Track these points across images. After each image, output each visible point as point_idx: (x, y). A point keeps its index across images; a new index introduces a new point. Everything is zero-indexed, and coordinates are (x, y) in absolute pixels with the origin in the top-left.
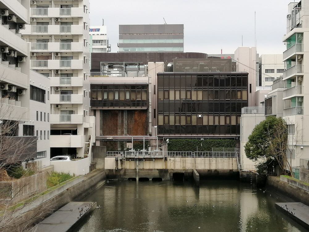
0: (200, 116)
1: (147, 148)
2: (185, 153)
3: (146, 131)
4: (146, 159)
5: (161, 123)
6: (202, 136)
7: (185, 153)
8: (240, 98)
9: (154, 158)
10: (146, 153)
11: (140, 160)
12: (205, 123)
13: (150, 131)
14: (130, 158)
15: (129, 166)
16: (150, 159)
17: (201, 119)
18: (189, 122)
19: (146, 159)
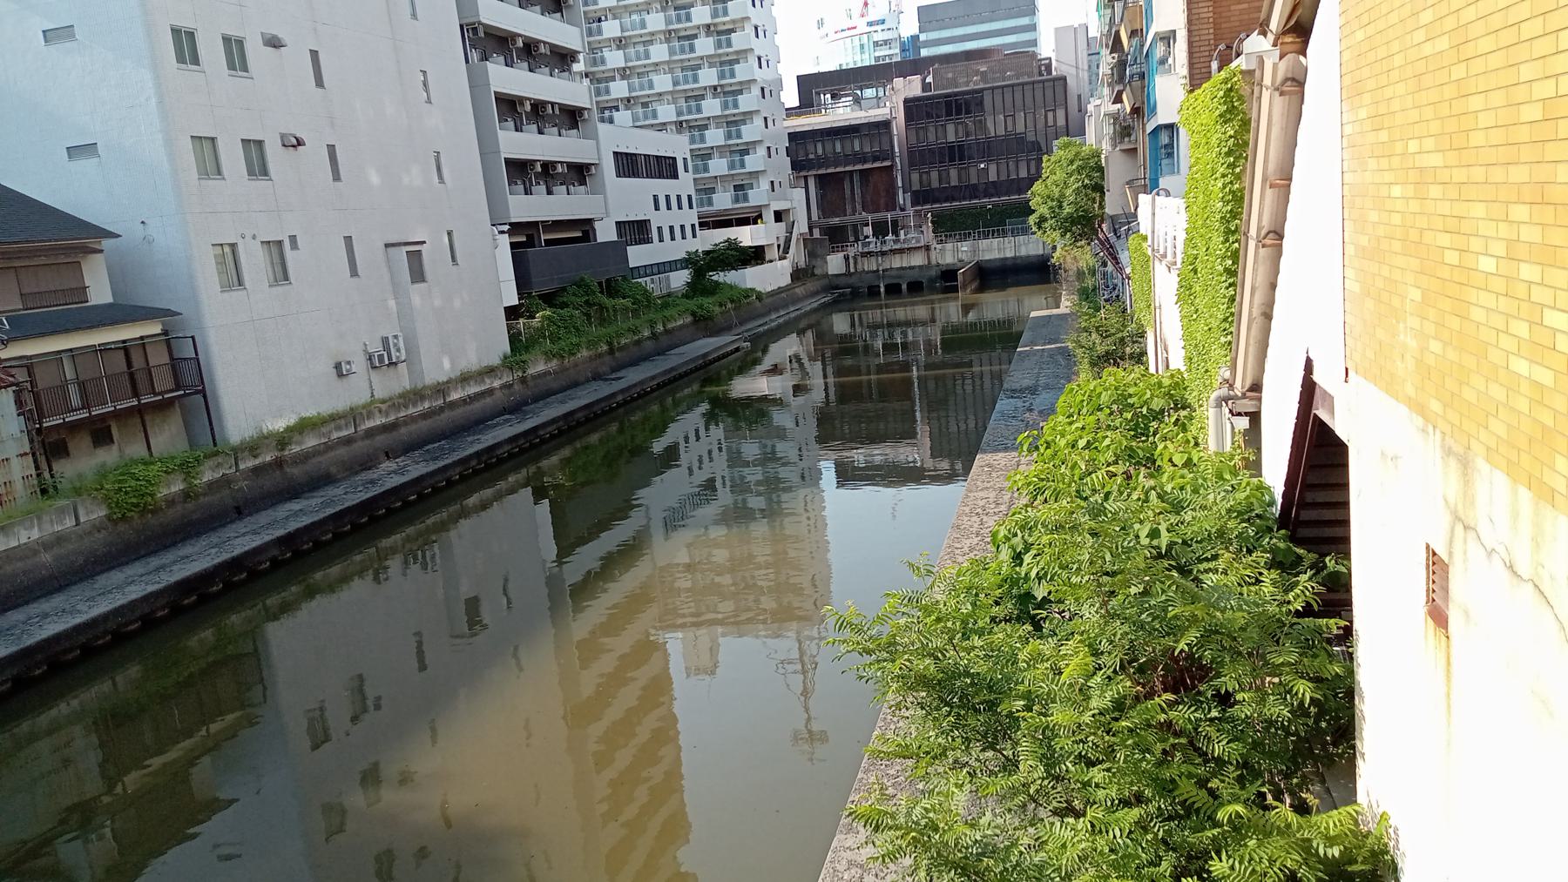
0: (982, 166)
1: (896, 233)
2: (998, 230)
3: (892, 205)
4: (894, 252)
5: (916, 187)
6: (988, 202)
7: (960, 234)
8: (171, 385)
9: (908, 249)
10: (895, 242)
11: (883, 253)
12: (993, 177)
13: (901, 202)
14: (869, 253)
15: (870, 265)
16: (901, 251)
17: (986, 170)
18: (925, 182)
19: (894, 252)
